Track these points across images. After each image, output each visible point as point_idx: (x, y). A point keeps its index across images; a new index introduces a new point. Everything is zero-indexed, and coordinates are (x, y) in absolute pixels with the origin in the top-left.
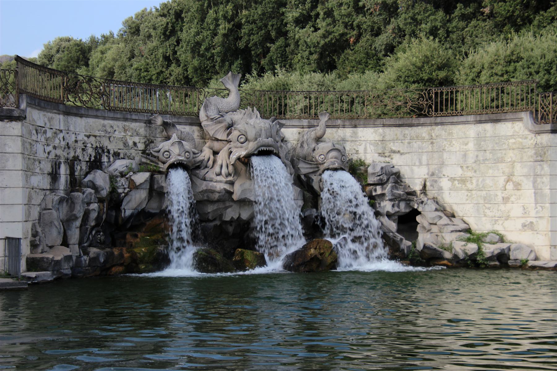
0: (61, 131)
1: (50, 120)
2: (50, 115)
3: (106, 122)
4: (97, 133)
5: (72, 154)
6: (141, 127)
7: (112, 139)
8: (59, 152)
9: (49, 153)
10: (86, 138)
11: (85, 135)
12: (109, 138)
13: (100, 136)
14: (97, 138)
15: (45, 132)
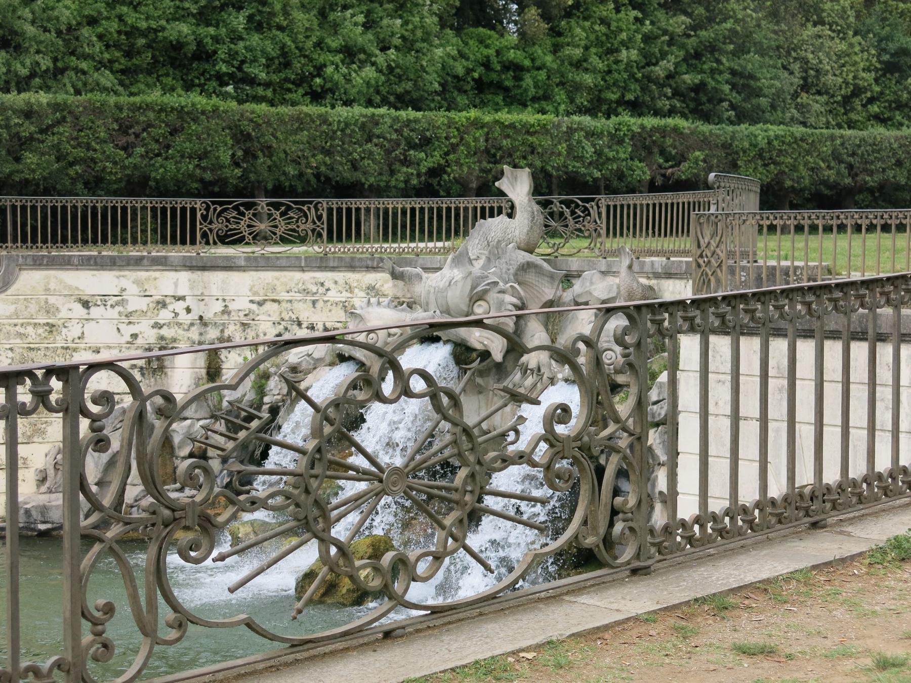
0: (182, 298)
1: (137, 282)
2: (142, 275)
3: (308, 276)
4: (284, 296)
5: (213, 334)
6: (386, 282)
7: (319, 305)
8: (165, 332)
9: (135, 336)
10: (254, 307)
11: (252, 302)
12: (314, 303)
13: (291, 301)
14: (284, 305)
15: (122, 303)
